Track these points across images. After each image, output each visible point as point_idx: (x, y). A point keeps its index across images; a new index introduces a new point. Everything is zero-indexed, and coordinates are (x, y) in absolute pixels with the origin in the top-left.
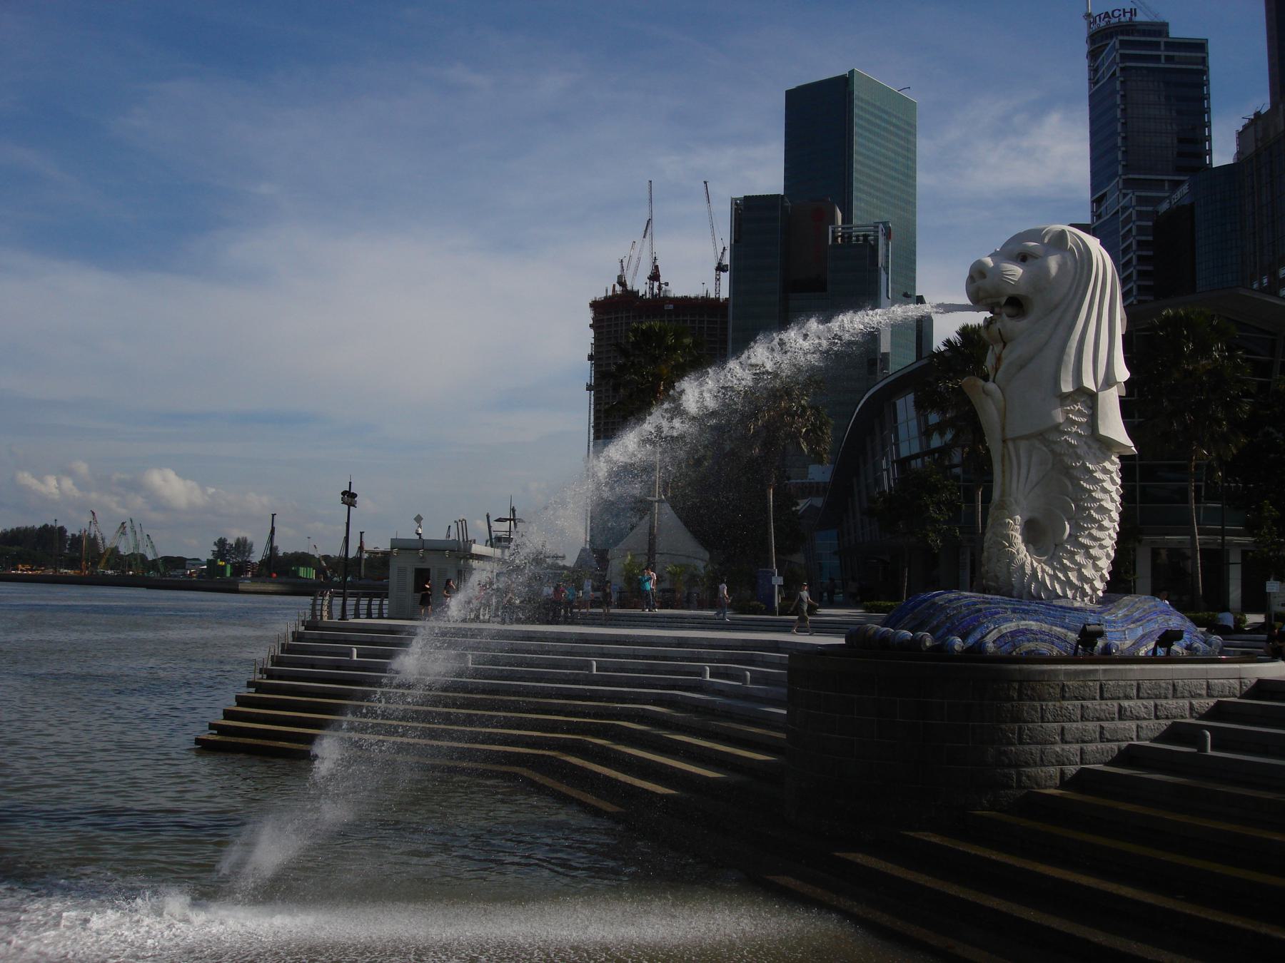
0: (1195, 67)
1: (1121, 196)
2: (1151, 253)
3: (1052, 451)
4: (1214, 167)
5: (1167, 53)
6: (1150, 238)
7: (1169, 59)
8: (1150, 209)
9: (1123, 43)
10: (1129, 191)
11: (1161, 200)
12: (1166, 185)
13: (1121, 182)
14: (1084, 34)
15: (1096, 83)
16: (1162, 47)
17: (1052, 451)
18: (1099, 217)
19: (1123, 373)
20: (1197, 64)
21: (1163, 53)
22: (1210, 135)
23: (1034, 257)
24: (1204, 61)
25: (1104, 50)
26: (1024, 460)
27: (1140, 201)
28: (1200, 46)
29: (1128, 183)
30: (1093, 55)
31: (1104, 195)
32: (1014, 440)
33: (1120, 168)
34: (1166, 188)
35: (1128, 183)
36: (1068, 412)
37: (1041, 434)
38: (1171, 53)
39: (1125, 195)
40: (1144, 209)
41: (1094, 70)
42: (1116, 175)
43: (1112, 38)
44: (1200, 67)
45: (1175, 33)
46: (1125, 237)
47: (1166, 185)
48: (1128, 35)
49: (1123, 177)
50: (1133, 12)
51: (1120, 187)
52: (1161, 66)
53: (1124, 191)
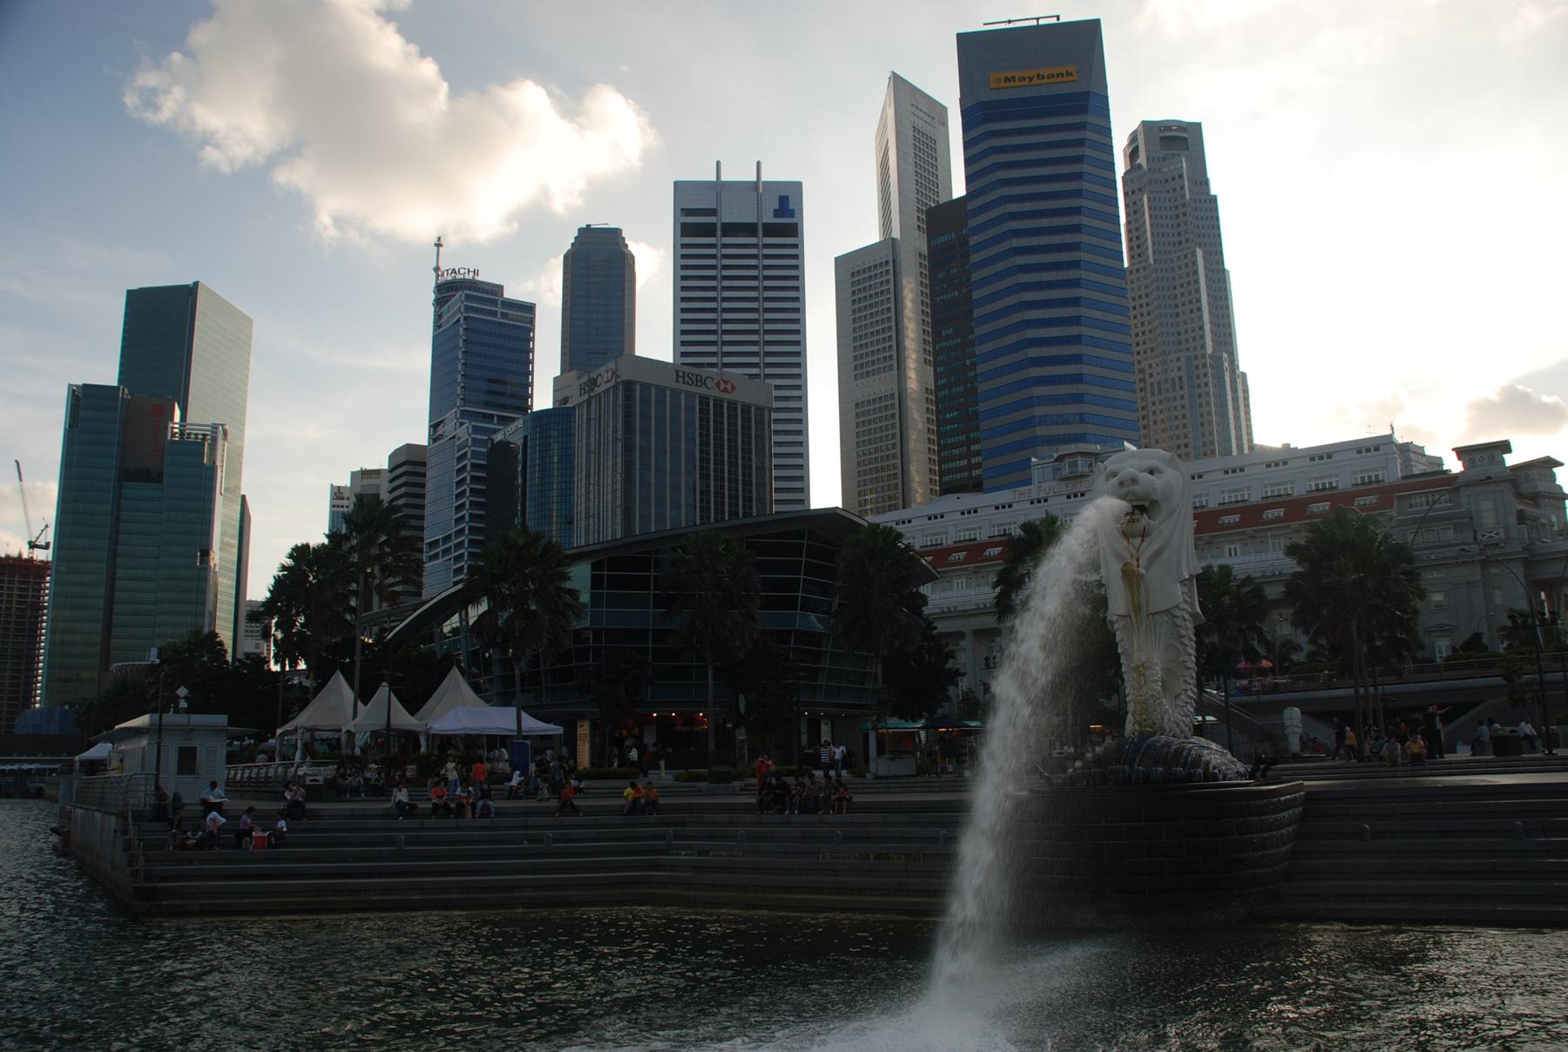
4: (536, 409)
7: (504, 315)
8: (486, 438)
9: (468, 297)
11: (495, 431)
12: (495, 418)
13: (458, 412)
14: (434, 285)
15: (440, 327)
18: (435, 440)
21: (500, 310)
22: (532, 382)
23: (1160, 472)
25: (448, 301)
26: (1158, 631)
27: (476, 430)
29: (464, 414)
30: (440, 302)
31: (442, 421)
33: (458, 402)
34: (495, 421)
35: (464, 414)
38: (506, 311)
39: (462, 424)
40: (478, 437)
41: (438, 317)
42: (454, 405)
43: (457, 290)
45: (508, 294)
47: (495, 418)
48: (470, 289)
50: (476, 272)
51: (458, 416)
53: (461, 420)
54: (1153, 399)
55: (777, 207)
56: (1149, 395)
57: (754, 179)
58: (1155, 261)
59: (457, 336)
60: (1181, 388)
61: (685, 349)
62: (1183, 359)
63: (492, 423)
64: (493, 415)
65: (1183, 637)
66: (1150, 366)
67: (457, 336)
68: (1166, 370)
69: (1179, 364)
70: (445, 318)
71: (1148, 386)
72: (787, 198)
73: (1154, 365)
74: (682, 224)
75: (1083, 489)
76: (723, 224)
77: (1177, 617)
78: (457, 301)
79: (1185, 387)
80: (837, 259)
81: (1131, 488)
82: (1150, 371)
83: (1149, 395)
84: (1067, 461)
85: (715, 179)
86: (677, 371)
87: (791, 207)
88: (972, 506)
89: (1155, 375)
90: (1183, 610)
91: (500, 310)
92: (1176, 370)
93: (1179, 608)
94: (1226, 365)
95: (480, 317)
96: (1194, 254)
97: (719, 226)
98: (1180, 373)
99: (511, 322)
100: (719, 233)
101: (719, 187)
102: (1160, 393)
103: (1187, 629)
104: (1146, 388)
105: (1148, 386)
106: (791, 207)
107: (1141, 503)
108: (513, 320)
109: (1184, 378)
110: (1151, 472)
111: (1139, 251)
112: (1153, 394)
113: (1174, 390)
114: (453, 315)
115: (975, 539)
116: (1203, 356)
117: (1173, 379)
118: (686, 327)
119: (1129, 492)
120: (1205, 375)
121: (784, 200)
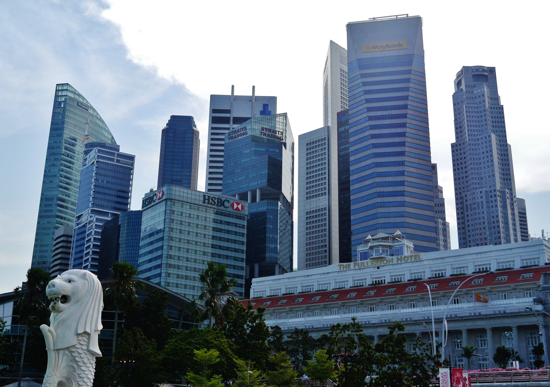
0: (128, 166)
1: (89, 217)
2: (99, 244)
3: (71, 355)
5: (117, 158)
6: (100, 237)
7: (118, 161)
8: (101, 224)
9: (99, 150)
10: (93, 215)
15: (85, 165)
16: (116, 154)
17: (71, 355)
19: (101, 327)
20: (129, 165)
21: (116, 158)
23: (74, 281)
24: (133, 164)
25: (90, 152)
28: (132, 158)
29: (93, 211)
30: (86, 153)
31: (82, 215)
32: (58, 350)
36: (79, 340)
37: (68, 348)
38: (119, 159)
39: (91, 217)
42: (88, 207)
44: (131, 167)
45: (122, 150)
46: (88, 235)
48: (102, 147)
49: (91, 208)
51: (90, 212)
52: (114, 163)
54: (467, 213)
55: (262, 110)
56: (465, 211)
57: (251, 95)
58: (469, 140)
59: (93, 171)
60: (483, 207)
61: (210, 182)
62: (483, 192)
63: (108, 216)
64: (109, 213)
65: (79, 362)
66: (466, 196)
67: (93, 171)
68: (474, 198)
69: (481, 195)
70: (87, 162)
71: (465, 206)
72: (267, 105)
73: (468, 195)
74: (213, 117)
76: (234, 118)
77: (74, 352)
78: (94, 153)
79: (485, 207)
80: (299, 136)
81: (53, 289)
82: (466, 198)
83: (465, 211)
84: (375, 249)
85: (230, 94)
86: (204, 196)
87: (269, 110)
89: (469, 200)
90: (78, 348)
91: (116, 158)
92: (480, 198)
93: (76, 348)
94: (508, 195)
95: (105, 161)
96: (490, 136)
97: (232, 119)
98: (482, 200)
99: (121, 165)
100: (231, 122)
101: (233, 99)
102: (471, 210)
103: (81, 358)
104: (463, 207)
105: (465, 206)
106: (269, 110)
107: (57, 296)
108: (122, 163)
109: (484, 202)
110: (70, 282)
111: (461, 134)
112: (467, 211)
113: (479, 208)
114: (91, 160)
115: (327, 290)
116: (495, 191)
117: (478, 203)
118: (212, 170)
119: (51, 291)
120: (496, 201)
121: (265, 106)
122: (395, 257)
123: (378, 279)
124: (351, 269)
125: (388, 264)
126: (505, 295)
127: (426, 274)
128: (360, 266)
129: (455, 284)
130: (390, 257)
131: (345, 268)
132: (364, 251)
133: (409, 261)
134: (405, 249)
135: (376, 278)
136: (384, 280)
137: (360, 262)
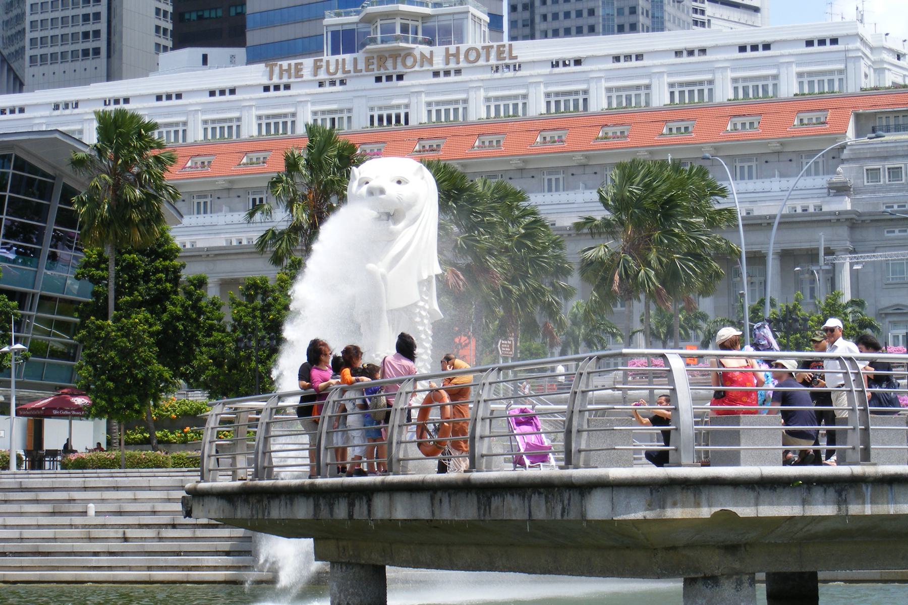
75: (400, 69)
84: (379, 23)
88: (227, 84)
122: (439, 51)
123: (389, 112)
124: (305, 78)
125: (417, 68)
126: (750, 167)
127: (531, 102)
128: (332, 69)
129: (622, 133)
130: (425, 49)
131: (285, 75)
132: (346, 27)
133: (482, 62)
134: (470, 26)
135: (380, 108)
136: (407, 115)
137: (327, 57)
